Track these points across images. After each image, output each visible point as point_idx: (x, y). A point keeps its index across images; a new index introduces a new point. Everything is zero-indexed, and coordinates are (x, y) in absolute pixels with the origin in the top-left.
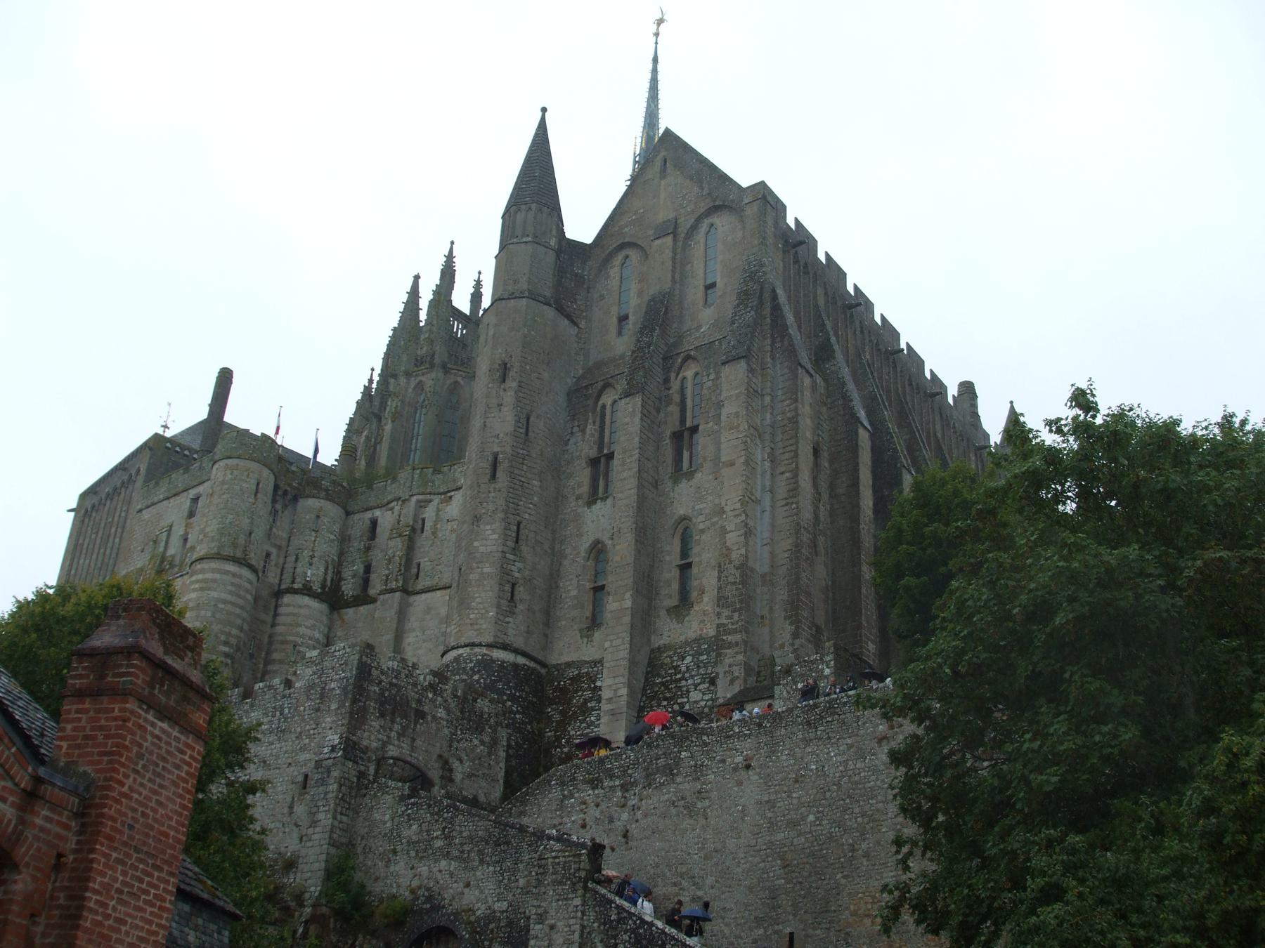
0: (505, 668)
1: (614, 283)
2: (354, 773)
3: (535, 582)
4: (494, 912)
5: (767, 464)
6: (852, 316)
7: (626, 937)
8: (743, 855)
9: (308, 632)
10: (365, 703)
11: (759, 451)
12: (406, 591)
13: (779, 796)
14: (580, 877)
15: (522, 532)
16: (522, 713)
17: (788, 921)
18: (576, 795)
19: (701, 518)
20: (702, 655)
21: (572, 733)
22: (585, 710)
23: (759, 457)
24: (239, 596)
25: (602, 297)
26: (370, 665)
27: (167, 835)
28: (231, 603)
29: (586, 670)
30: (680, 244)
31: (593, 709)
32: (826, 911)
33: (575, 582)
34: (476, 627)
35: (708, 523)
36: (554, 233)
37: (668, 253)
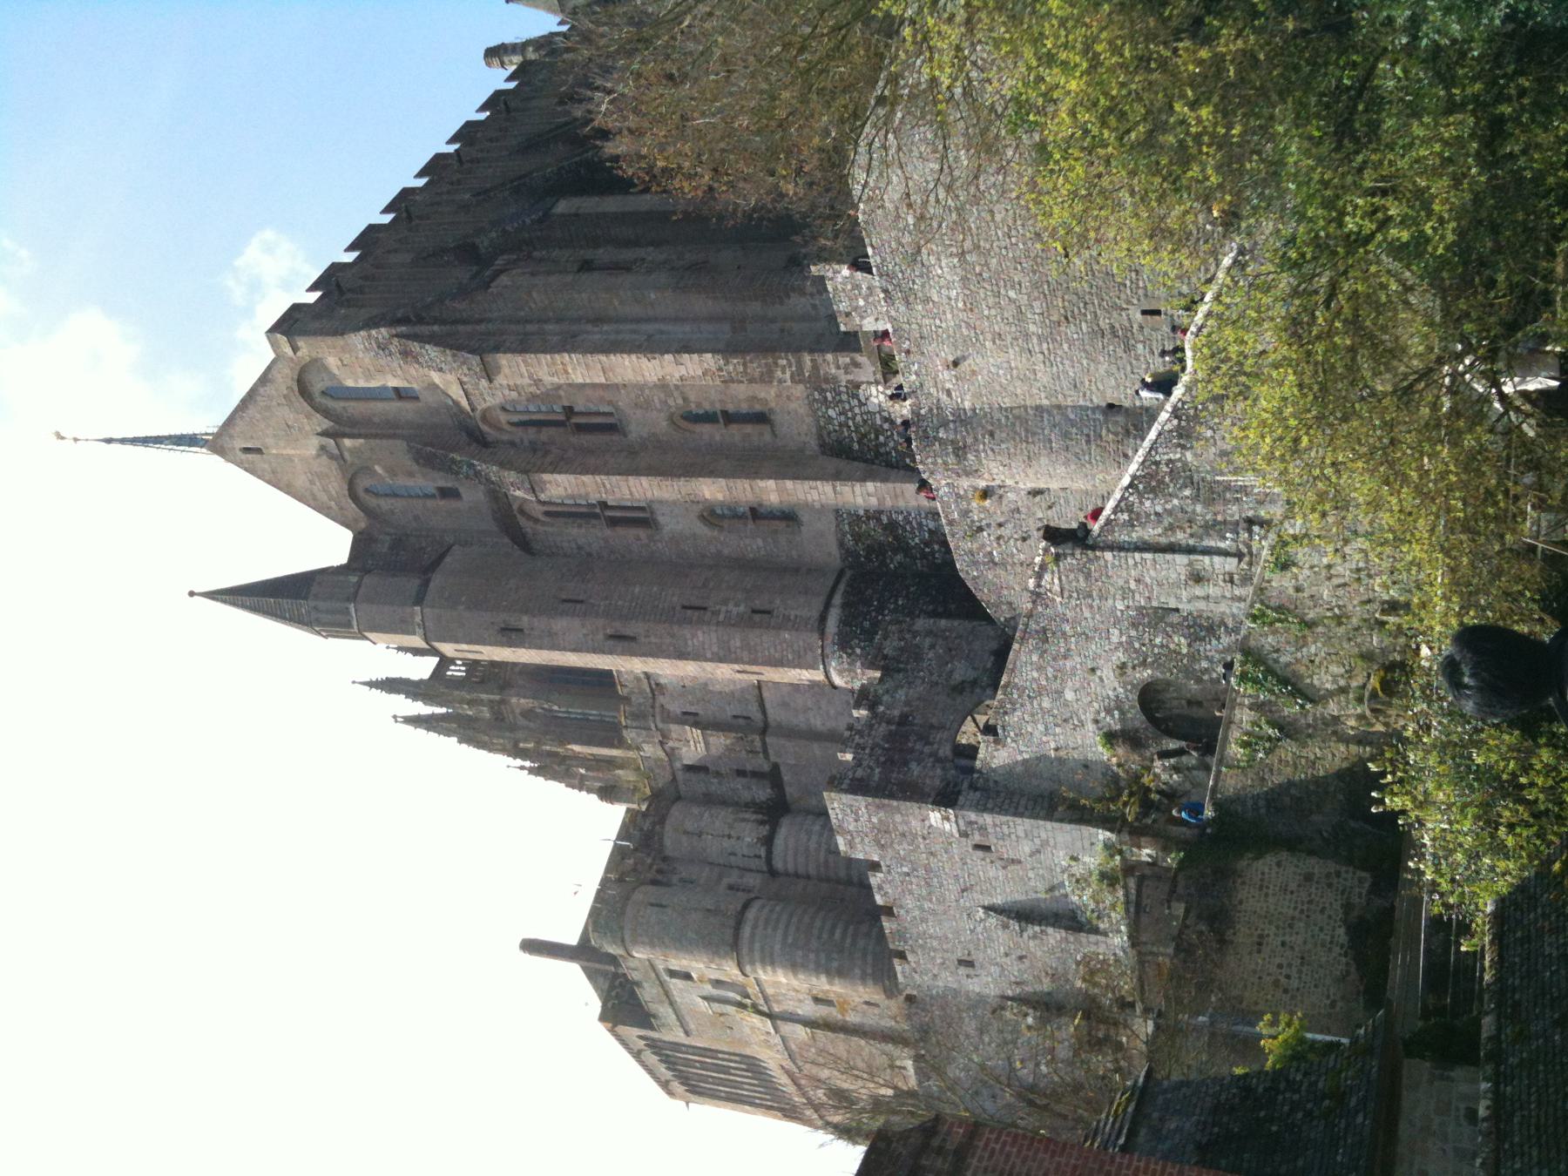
1: (398, 504)
3: (749, 586)
4: (1121, 643)
7: (1148, 503)
8: (1055, 368)
9: (814, 838)
12: (764, 730)
16: (897, 597)
18: (989, 549)
19: (671, 402)
20: (826, 398)
21: (917, 540)
22: (892, 526)
23: (597, 337)
24: (778, 921)
25: (416, 518)
27: (1075, 1167)
28: (787, 926)
29: (847, 527)
30: (347, 430)
31: (890, 518)
33: (747, 541)
35: (676, 394)
36: (342, 578)
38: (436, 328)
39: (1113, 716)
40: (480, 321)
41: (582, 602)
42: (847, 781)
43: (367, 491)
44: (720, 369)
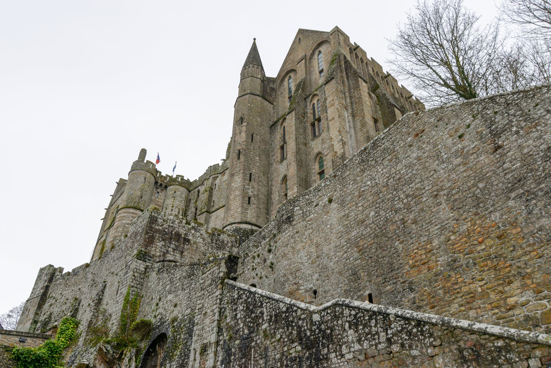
0: (247, 231)
2: (143, 266)
5: (350, 117)
6: (387, 82)
7: (241, 308)
8: (333, 254)
10: (153, 234)
11: (346, 112)
13: (351, 209)
14: (219, 277)
15: (253, 177)
17: (366, 286)
18: (250, 255)
19: (326, 150)
23: (346, 115)
25: (282, 93)
26: (157, 217)
30: (308, 62)
32: (392, 271)
33: (277, 194)
34: (233, 217)
35: (328, 151)
37: (303, 66)
38: (343, 66)
39: (159, 322)
40: (348, 79)
41: (252, 141)
42: (156, 215)
43: (290, 77)
44: (337, 157)
